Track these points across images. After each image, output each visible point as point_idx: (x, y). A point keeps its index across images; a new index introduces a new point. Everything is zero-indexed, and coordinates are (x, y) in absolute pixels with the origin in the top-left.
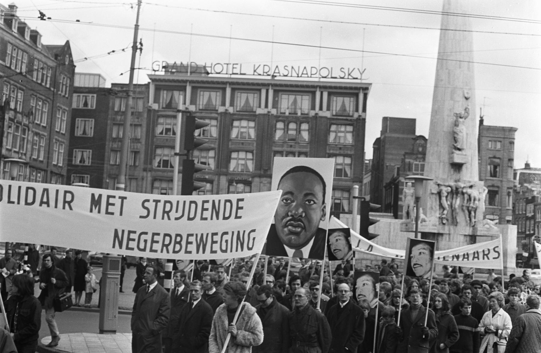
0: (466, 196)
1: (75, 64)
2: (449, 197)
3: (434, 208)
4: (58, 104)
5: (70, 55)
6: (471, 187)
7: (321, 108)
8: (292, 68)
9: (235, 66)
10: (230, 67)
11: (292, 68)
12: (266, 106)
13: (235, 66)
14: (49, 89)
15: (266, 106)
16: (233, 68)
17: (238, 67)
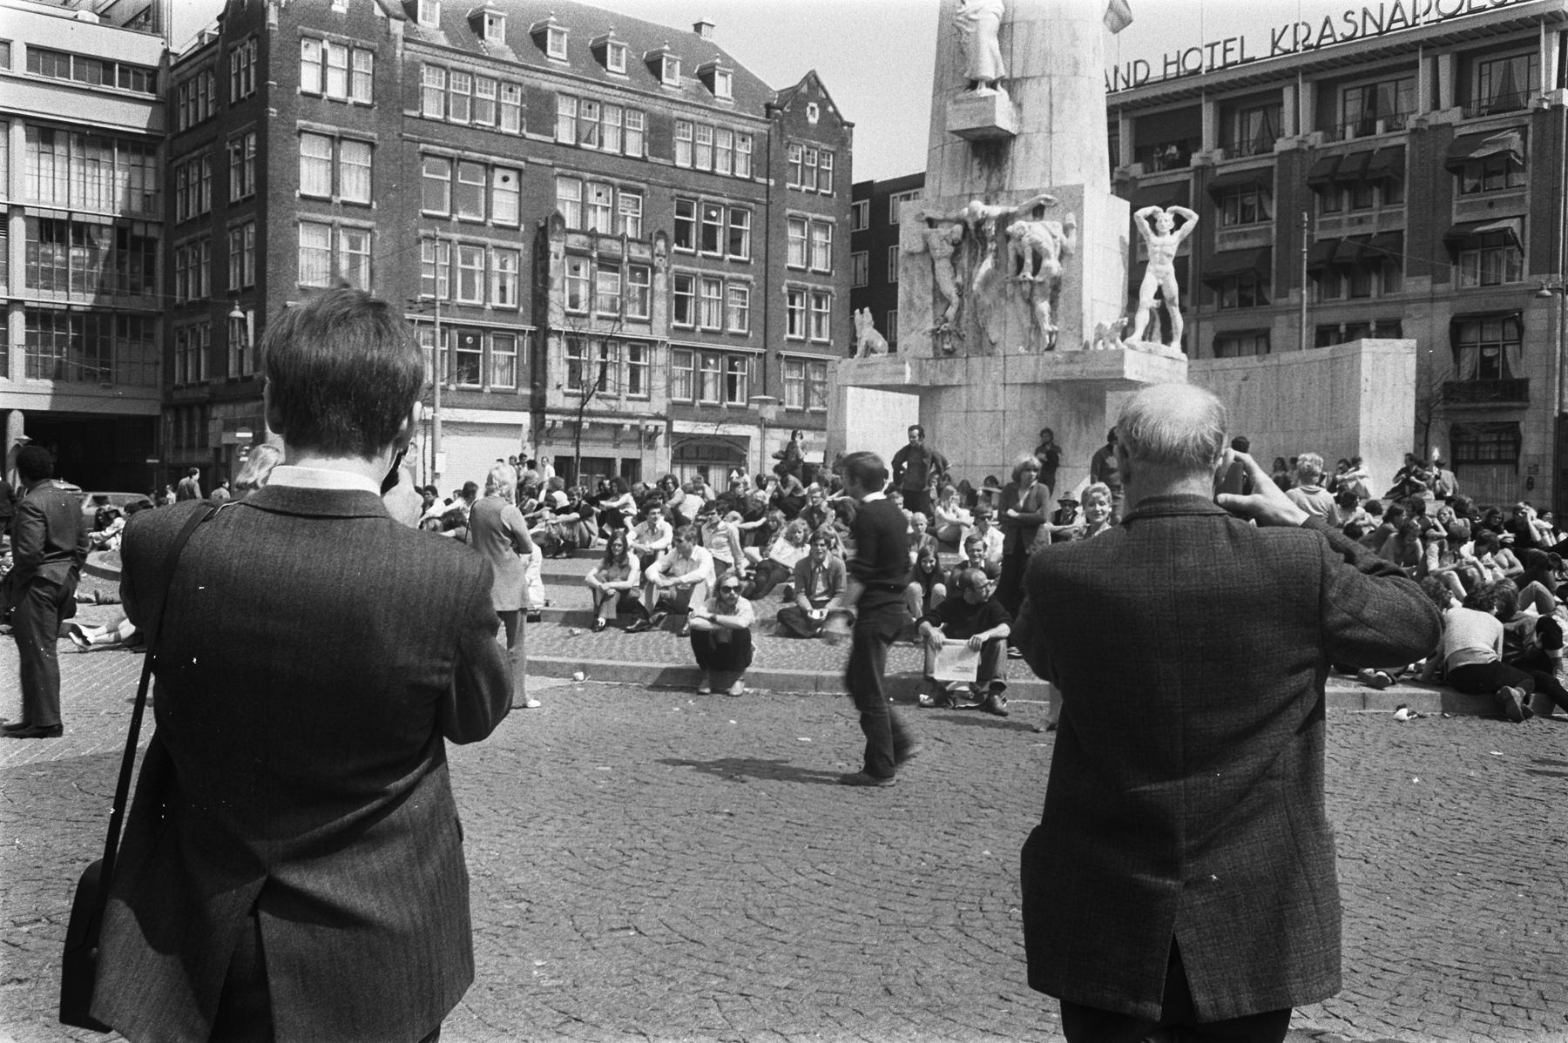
0: (1011, 245)
1: (846, 119)
2: (965, 261)
3: (916, 301)
4: (789, 211)
5: (826, 102)
6: (1038, 211)
7: (1436, 105)
8: (1365, 13)
9: (1229, 45)
10: (1219, 49)
11: (1365, 13)
12: (1297, 131)
13: (1229, 45)
14: (751, 181)
15: (1297, 131)
16: (1226, 51)
17: (1236, 45)
